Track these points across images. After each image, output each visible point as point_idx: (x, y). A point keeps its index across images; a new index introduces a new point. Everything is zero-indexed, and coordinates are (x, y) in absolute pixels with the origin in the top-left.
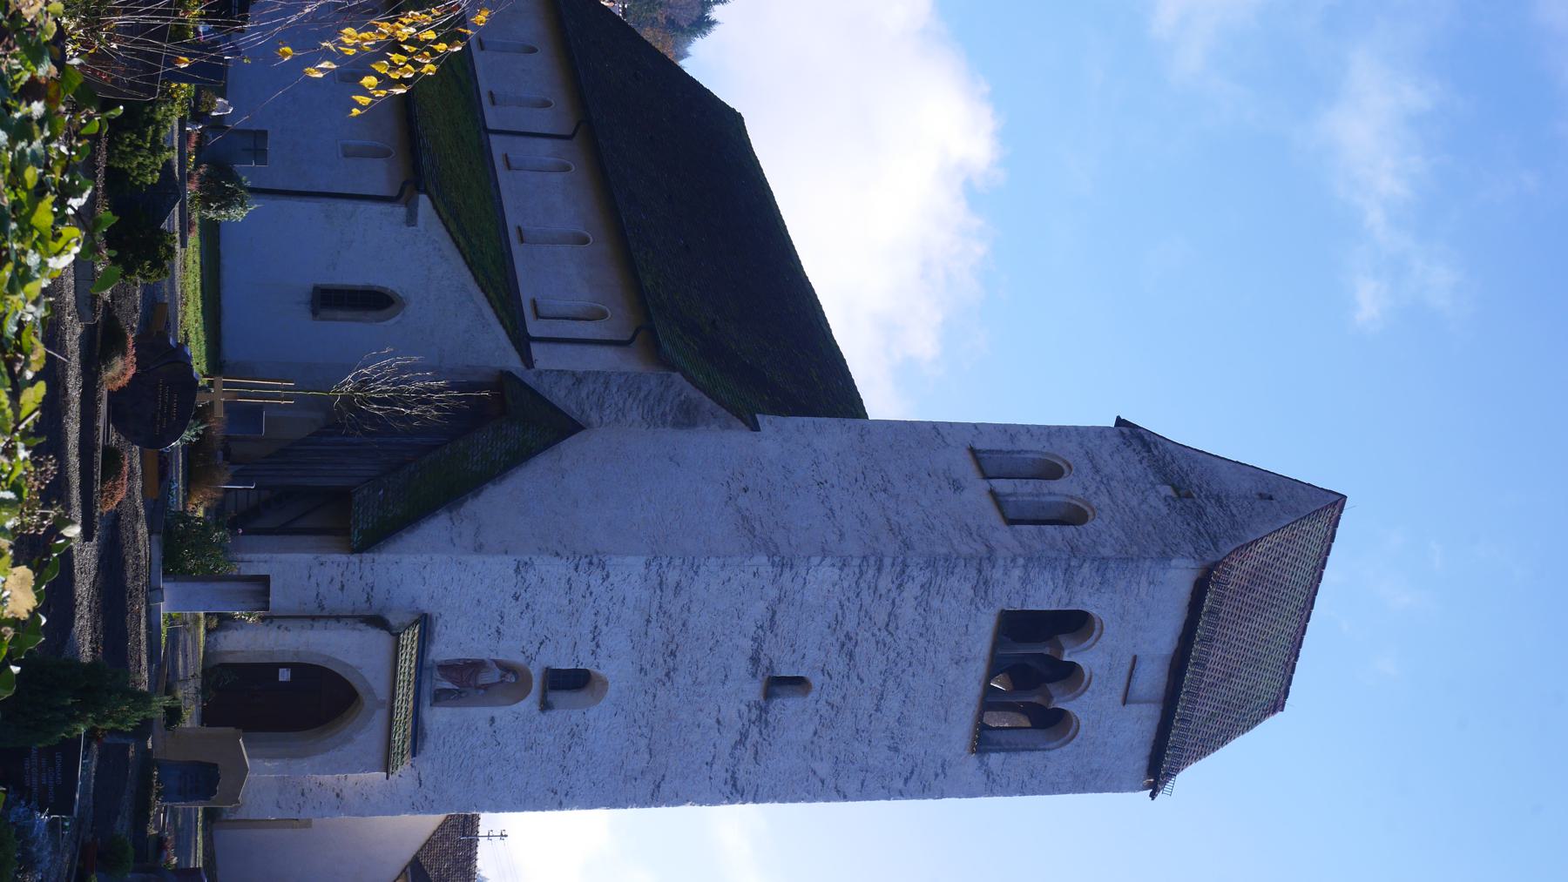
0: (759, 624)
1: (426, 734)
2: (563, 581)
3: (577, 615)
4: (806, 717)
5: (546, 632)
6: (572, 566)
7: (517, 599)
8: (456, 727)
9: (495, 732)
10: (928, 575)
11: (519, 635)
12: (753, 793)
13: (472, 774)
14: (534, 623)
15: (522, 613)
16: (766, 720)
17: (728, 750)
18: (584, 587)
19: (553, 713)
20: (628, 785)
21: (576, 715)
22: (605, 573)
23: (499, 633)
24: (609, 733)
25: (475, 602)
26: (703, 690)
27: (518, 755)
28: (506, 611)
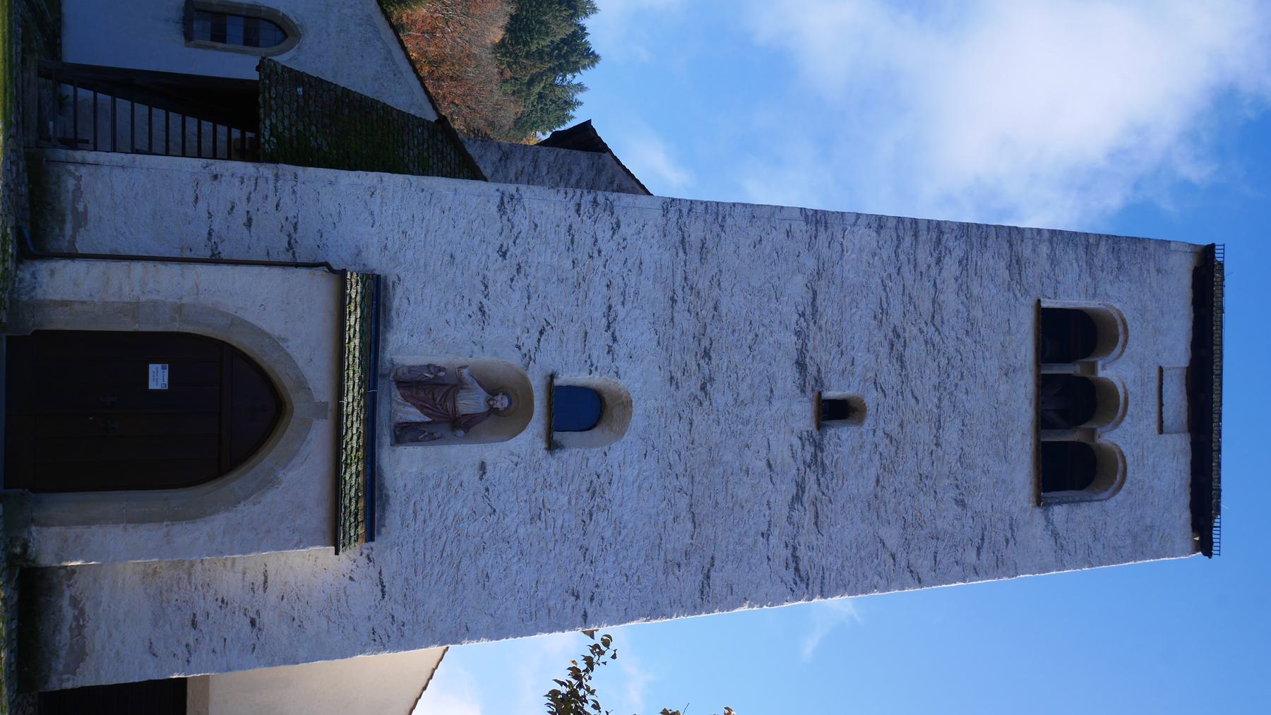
0: (801, 309)
1: (387, 496)
2: (563, 230)
3: (584, 286)
4: (865, 456)
5: (546, 314)
6: (572, 206)
7: (504, 255)
8: (431, 483)
9: (487, 490)
10: (963, 246)
11: (511, 317)
12: (819, 581)
13: (458, 567)
14: (529, 298)
15: (512, 280)
16: (822, 462)
17: (785, 511)
18: (590, 241)
19: (565, 455)
20: (671, 578)
21: (594, 456)
22: (614, 221)
23: (484, 313)
24: (640, 487)
25: (447, 258)
26: (746, 413)
27: (522, 531)
28: (490, 274)
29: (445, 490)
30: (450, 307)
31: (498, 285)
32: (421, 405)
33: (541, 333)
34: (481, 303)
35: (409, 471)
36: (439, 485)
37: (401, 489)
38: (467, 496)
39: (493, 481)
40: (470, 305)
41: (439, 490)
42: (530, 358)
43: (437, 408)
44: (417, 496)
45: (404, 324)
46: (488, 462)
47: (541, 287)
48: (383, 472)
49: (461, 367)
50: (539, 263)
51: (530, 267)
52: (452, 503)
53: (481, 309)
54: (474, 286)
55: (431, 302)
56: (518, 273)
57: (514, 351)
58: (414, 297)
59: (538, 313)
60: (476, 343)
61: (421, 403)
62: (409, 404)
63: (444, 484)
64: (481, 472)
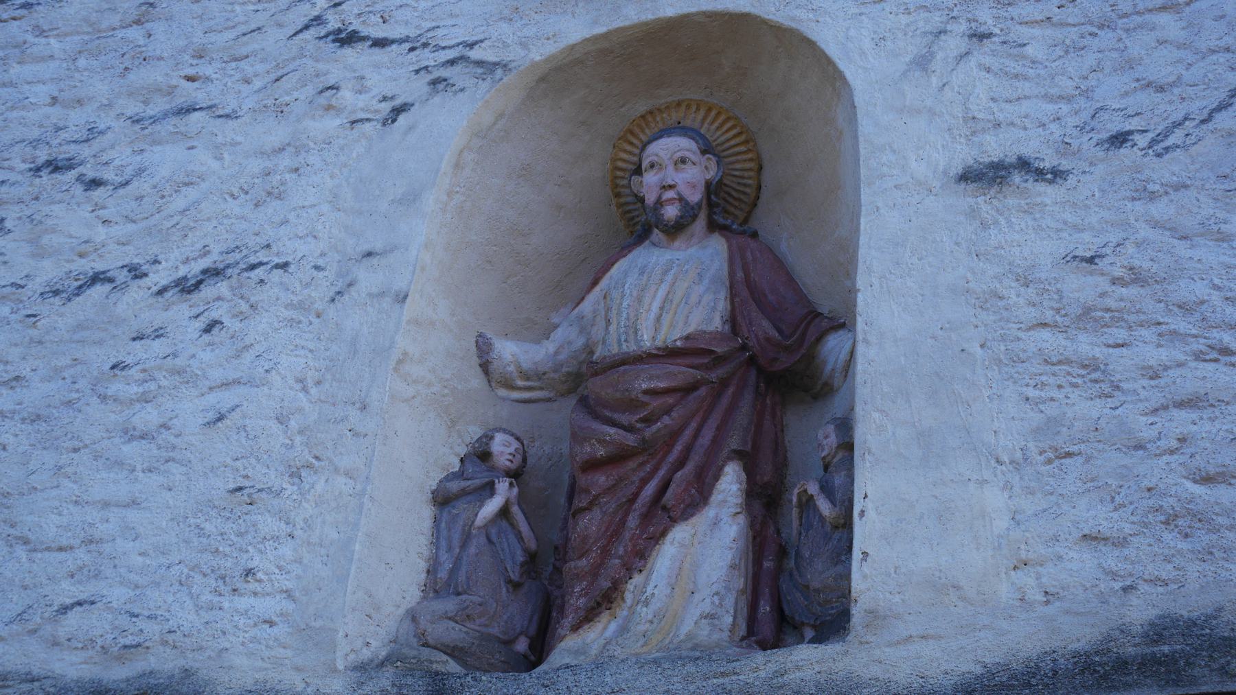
1: (1158, 631)
5: (273, 40)
9: (1120, 139)
15: (95, 183)
28: (48, 272)
29: (1121, 334)
30: (148, 417)
31: (101, 233)
32: (647, 517)
33: (347, 38)
34: (160, 292)
35: (1002, 523)
36: (1091, 365)
37: (1111, 558)
38: (1155, 225)
39: (1072, 121)
40: (158, 334)
41: (1122, 363)
42: (452, 62)
43: (674, 435)
44: (1154, 471)
45: (186, 617)
46: (964, 155)
47: (153, 75)
48: (1005, 667)
49: (485, 367)
50: (54, 100)
51: (58, 129)
52: (1201, 290)
53: (187, 287)
54: (80, 327)
55: (106, 505)
56: (71, 167)
57: (411, 128)
58: (65, 585)
59: (260, 68)
60: (340, 285)
61: (633, 521)
62: (637, 579)
63: (1086, 345)
64: (1017, 178)
